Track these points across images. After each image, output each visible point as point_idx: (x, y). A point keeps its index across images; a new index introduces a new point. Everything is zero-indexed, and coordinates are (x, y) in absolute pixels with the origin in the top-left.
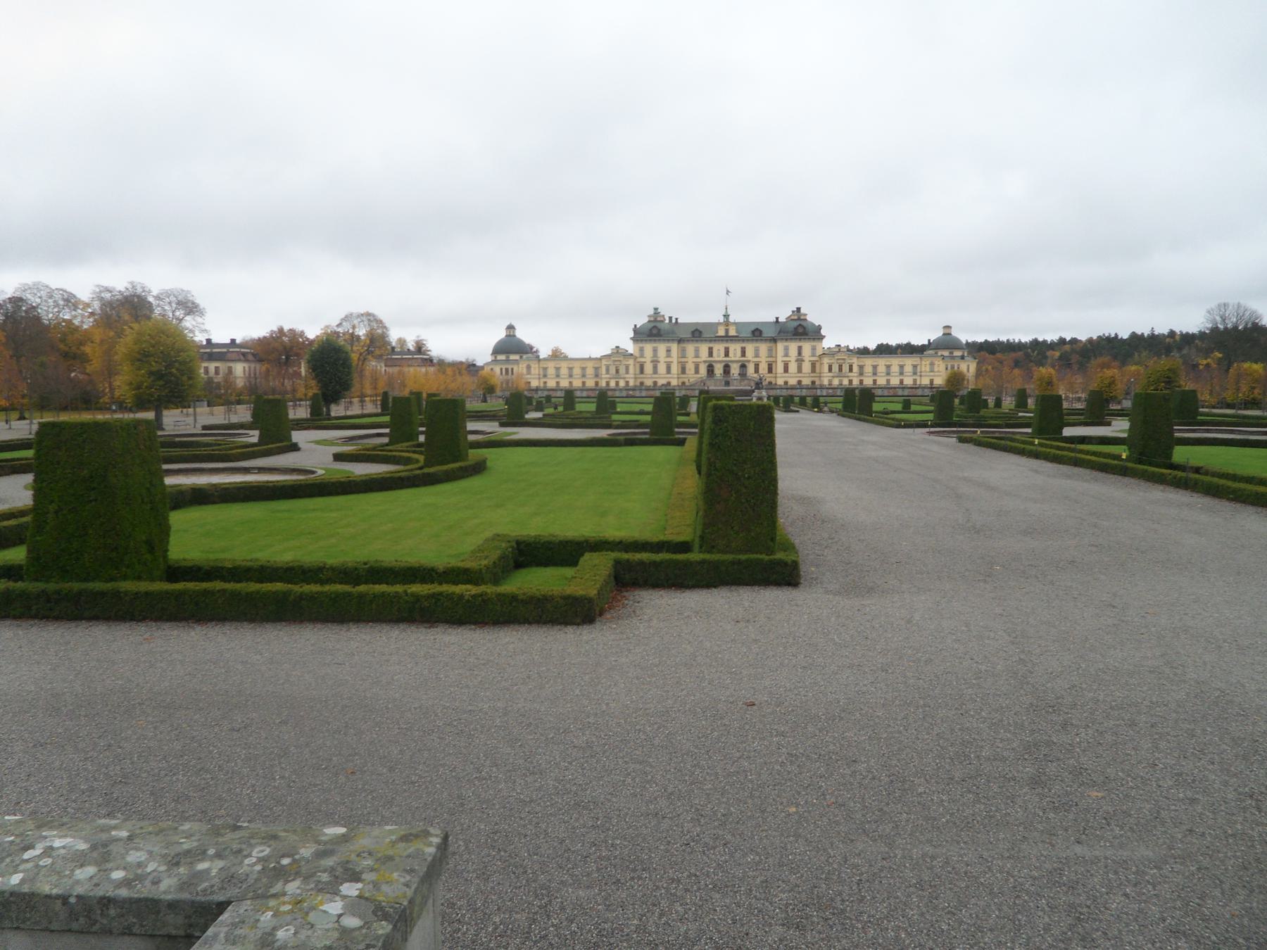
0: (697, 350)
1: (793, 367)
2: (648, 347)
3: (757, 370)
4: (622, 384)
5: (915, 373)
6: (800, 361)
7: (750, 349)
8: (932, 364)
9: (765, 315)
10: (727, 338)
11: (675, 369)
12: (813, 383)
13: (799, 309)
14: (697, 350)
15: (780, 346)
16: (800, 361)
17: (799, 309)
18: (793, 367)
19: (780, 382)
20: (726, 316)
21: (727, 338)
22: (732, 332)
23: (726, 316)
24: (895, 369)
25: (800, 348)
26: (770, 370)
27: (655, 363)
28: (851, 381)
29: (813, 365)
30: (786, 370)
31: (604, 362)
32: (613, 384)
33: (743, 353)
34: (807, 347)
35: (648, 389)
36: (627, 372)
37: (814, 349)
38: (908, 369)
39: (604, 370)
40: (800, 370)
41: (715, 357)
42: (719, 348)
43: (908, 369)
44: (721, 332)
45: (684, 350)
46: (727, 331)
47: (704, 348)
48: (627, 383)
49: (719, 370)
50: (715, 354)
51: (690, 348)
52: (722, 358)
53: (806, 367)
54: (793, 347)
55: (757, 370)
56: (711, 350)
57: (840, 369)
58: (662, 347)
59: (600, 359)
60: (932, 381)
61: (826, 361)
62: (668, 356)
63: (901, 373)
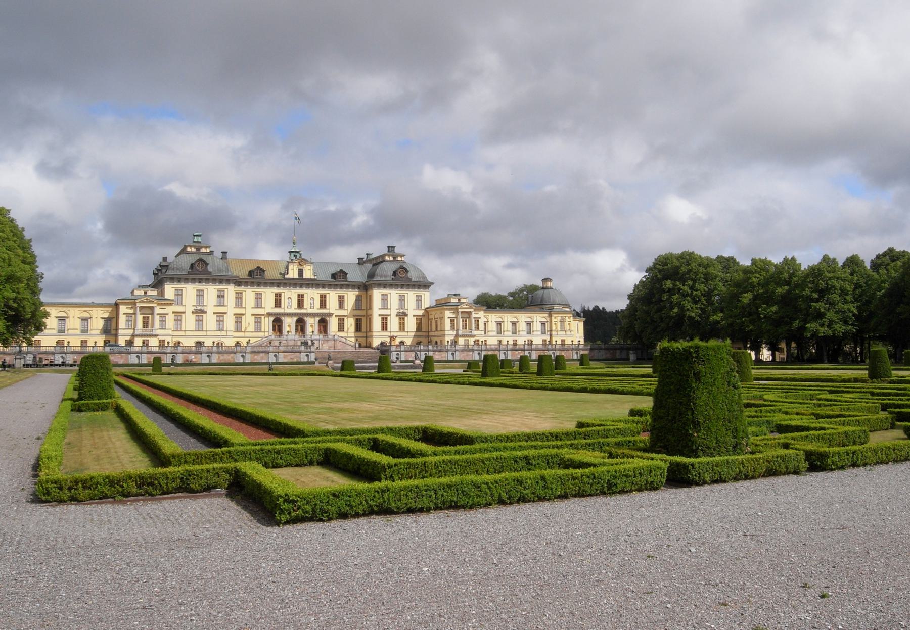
0: (258, 297)
2: (190, 290)
3: (341, 328)
4: (154, 342)
5: (544, 333)
6: (402, 316)
7: (332, 296)
8: (563, 322)
10: (301, 282)
11: (229, 322)
13: (391, 248)
14: (258, 297)
16: (402, 316)
17: (391, 248)
19: (376, 342)
22: (308, 274)
24: (522, 326)
25: (402, 299)
26: (358, 328)
27: (199, 312)
30: (384, 327)
31: (123, 309)
32: (138, 342)
33: (323, 304)
34: (411, 295)
36: (163, 327)
37: (419, 299)
38: (537, 326)
41: (284, 309)
42: (290, 295)
43: (537, 326)
44: (293, 273)
45: (239, 297)
46: (301, 272)
47: (269, 294)
48: (162, 342)
49: (289, 324)
50: (284, 302)
51: (249, 293)
52: (294, 309)
53: (411, 324)
54: (394, 295)
55: (341, 328)
57: (465, 327)
58: (211, 291)
61: (448, 314)
62: (220, 304)
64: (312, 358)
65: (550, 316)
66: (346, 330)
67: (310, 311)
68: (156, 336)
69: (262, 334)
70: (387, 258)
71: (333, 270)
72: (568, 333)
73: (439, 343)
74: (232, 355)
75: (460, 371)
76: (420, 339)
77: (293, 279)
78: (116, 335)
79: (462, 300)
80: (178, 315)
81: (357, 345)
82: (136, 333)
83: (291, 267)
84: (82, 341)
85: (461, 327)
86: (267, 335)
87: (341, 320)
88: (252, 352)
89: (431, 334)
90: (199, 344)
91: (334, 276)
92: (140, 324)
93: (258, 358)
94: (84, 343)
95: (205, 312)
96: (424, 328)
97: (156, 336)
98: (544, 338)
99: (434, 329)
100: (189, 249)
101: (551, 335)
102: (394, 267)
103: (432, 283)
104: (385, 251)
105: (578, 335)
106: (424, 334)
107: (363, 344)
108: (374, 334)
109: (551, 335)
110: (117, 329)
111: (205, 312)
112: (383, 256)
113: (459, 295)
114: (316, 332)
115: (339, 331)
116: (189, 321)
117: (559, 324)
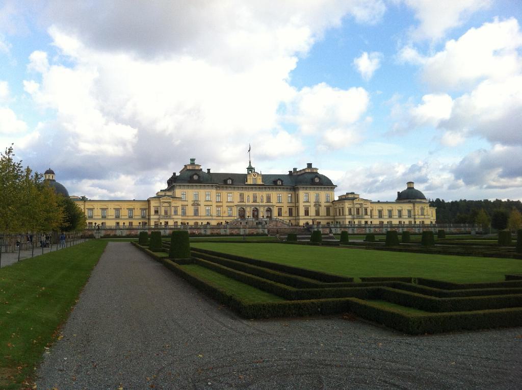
1: (312, 212)
3: (280, 215)
4: (171, 223)
5: (410, 216)
6: (317, 204)
7: (275, 195)
8: (422, 209)
9: (282, 169)
10: (255, 186)
12: (328, 223)
13: (310, 165)
15: (302, 194)
17: (310, 165)
18: (312, 212)
19: (302, 223)
20: (250, 169)
21: (255, 186)
22: (260, 182)
23: (250, 169)
25: (318, 196)
26: (291, 214)
28: (366, 222)
29: (328, 209)
30: (307, 213)
31: (153, 204)
34: (323, 195)
35: (213, 228)
37: (327, 197)
38: (405, 213)
39: (152, 212)
40: (317, 213)
42: (249, 194)
43: (405, 213)
44: (250, 181)
49: (249, 213)
53: (323, 211)
56: (242, 196)
57: (358, 213)
59: (148, 201)
60: (423, 222)
63: (400, 216)
64: (266, 231)
65: (414, 206)
66: (283, 215)
67: (261, 204)
68: (173, 219)
69: (233, 218)
70: (307, 171)
71: (273, 179)
72: (426, 217)
73: (341, 223)
74: (218, 230)
75: (361, 241)
76: (328, 221)
77: (250, 185)
78: (149, 219)
79: (356, 197)
80: (184, 207)
81: (290, 224)
82: (161, 217)
83: (248, 177)
84: (130, 223)
85: (356, 213)
86: (236, 218)
87: (280, 210)
88: (230, 228)
89: (336, 217)
90: (196, 224)
91: (275, 182)
92: (163, 213)
93: (234, 232)
94: (131, 224)
95: (200, 205)
96: (332, 214)
97: (173, 219)
98: (410, 220)
99: (338, 214)
100: (188, 168)
101: (415, 218)
102: (313, 176)
103: (336, 186)
104: (306, 166)
105: (432, 218)
106: (331, 218)
107: (294, 224)
108: (300, 218)
109: (415, 218)
110: (149, 215)
111: (200, 205)
112: (304, 170)
113: (353, 193)
114: (265, 217)
115: (279, 215)
116: (190, 211)
117: (420, 211)
